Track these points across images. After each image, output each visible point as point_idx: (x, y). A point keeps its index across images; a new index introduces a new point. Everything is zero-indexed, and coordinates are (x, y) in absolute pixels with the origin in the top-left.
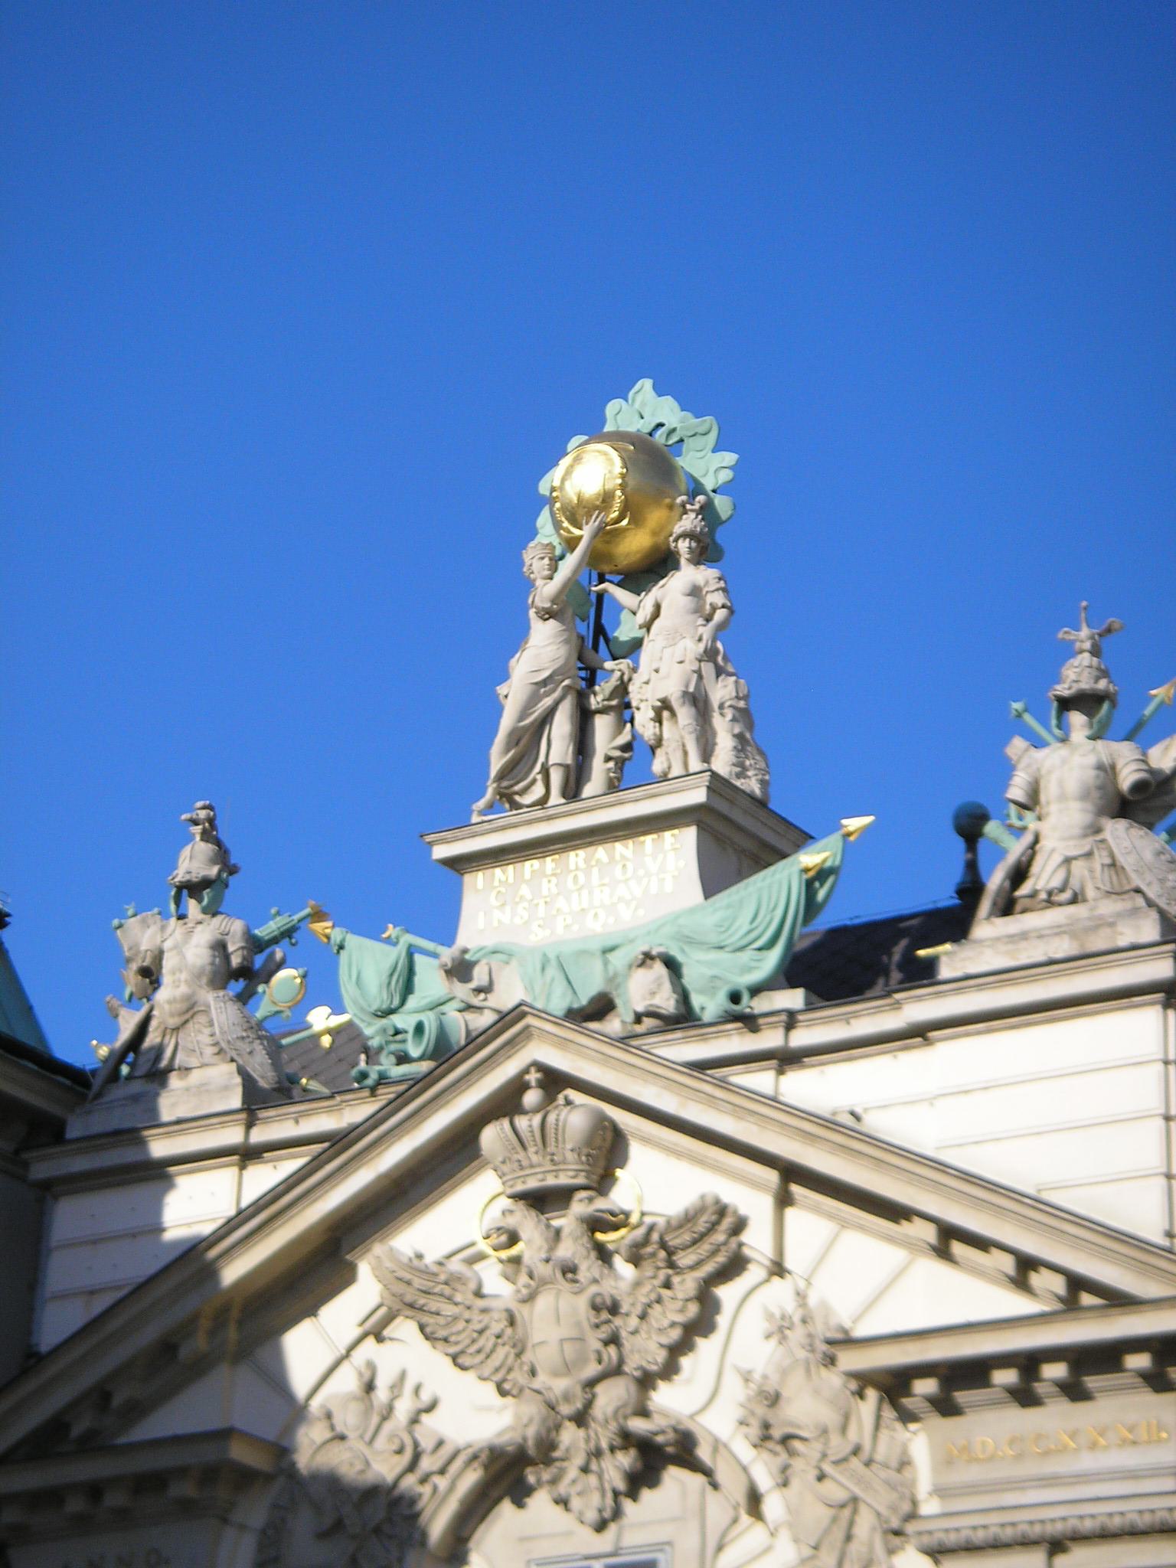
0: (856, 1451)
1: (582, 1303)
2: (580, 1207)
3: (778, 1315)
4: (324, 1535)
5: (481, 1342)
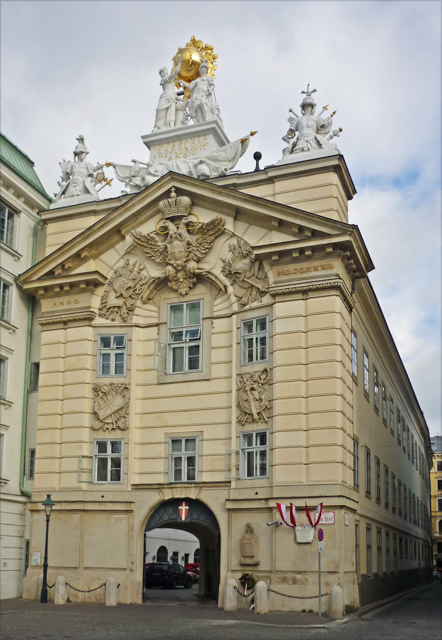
1: (185, 243)
2: (183, 221)
3: (233, 246)
4: (116, 297)
5: (157, 254)
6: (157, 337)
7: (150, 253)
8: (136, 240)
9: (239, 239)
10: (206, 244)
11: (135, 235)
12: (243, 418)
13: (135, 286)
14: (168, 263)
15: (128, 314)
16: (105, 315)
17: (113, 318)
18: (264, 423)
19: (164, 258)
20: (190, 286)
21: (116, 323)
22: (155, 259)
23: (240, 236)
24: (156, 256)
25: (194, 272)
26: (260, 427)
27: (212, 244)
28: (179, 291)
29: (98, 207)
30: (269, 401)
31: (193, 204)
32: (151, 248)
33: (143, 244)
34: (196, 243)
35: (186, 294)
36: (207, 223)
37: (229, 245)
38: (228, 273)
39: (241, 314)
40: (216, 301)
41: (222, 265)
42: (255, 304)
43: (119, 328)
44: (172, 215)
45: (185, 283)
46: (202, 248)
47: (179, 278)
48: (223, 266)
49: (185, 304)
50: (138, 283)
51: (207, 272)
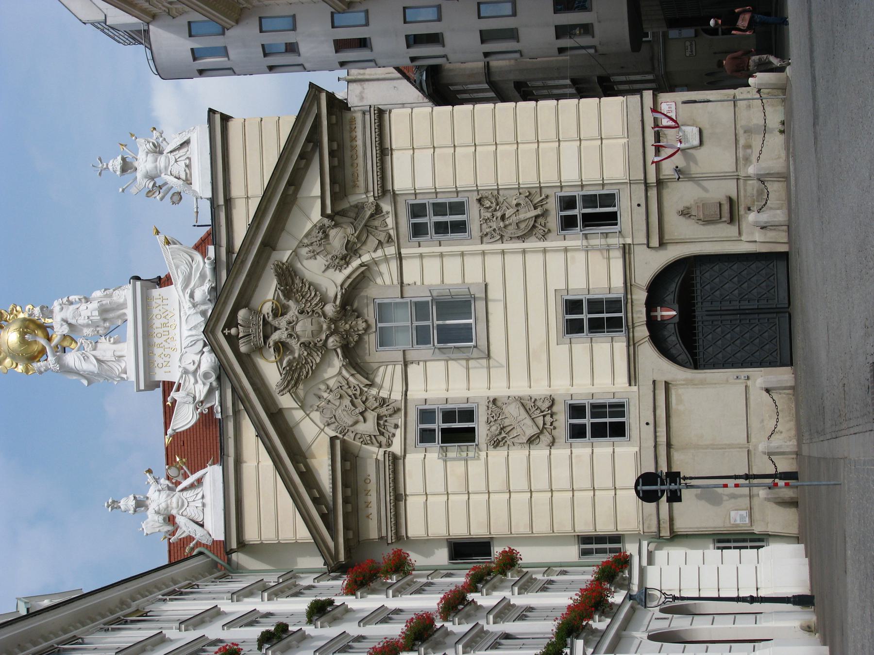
0: (352, 223)
1: (301, 317)
4: (365, 421)
5: (310, 361)
6: (421, 363)
8: (290, 387)
9: (301, 245)
11: (282, 387)
12: (539, 231)
13: (350, 396)
15: (388, 405)
17: (393, 426)
18: (548, 201)
21: (400, 422)
22: (317, 364)
23: (297, 243)
24: (312, 362)
26: (552, 205)
27: (305, 280)
28: (360, 333)
29: (230, 455)
30: (520, 194)
39: (401, 241)
41: (331, 271)
42: (390, 221)
46: (309, 295)
48: (333, 270)
49: (380, 325)
51: (342, 288)
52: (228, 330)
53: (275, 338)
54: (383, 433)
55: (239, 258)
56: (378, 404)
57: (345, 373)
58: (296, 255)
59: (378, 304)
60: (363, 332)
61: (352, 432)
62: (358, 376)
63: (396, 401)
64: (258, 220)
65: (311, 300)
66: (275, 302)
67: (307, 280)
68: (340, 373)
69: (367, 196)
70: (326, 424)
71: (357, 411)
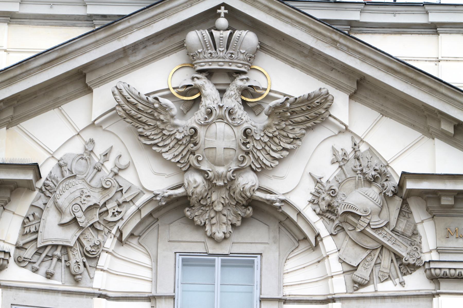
1: (239, 132)
2: (239, 83)
3: (341, 153)
4: (62, 225)
5: (167, 142)
7: (152, 137)
8: (126, 107)
10: (284, 140)
11: (125, 93)
13: (105, 204)
14: (190, 165)
15: (85, 266)
16: (30, 262)
17: (51, 270)
19: (184, 153)
20: (234, 222)
21: (56, 283)
24: (165, 146)
25: (252, 196)
27: (298, 142)
28: (208, 228)
31: (262, 47)
32: (156, 127)
33: (139, 116)
34: (262, 135)
35: (225, 238)
36: (296, 99)
37: (334, 149)
38: (327, 209)
40: (288, 262)
41: (312, 187)
43: (60, 295)
44: (215, 66)
45: (225, 215)
46: (274, 148)
47: (213, 203)
49: (218, 260)
50: (111, 199)
51: (283, 201)
52: (225, 14)
53: (207, 88)
54: (41, 254)
55: (341, 36)
56: (89, 249)
57: (146, 197)
58: (340, 132)
59: (253, 261)
60: (209, 234)
61: (45, 204)
62: (137, 221)
63: (92, 278)
64: (402, 71)
65: (266, 151)
66: (266, 93)
67: (299, 146)
68: (144, 190)
69: (431, 251)
70: (61, 162)
71: (79, 214)
